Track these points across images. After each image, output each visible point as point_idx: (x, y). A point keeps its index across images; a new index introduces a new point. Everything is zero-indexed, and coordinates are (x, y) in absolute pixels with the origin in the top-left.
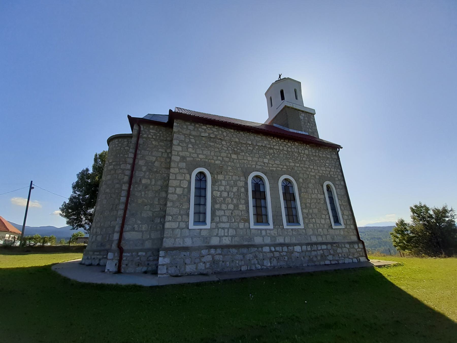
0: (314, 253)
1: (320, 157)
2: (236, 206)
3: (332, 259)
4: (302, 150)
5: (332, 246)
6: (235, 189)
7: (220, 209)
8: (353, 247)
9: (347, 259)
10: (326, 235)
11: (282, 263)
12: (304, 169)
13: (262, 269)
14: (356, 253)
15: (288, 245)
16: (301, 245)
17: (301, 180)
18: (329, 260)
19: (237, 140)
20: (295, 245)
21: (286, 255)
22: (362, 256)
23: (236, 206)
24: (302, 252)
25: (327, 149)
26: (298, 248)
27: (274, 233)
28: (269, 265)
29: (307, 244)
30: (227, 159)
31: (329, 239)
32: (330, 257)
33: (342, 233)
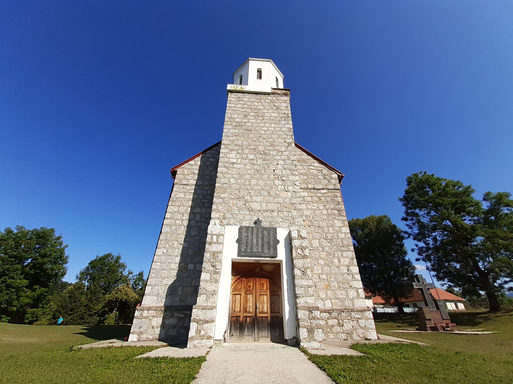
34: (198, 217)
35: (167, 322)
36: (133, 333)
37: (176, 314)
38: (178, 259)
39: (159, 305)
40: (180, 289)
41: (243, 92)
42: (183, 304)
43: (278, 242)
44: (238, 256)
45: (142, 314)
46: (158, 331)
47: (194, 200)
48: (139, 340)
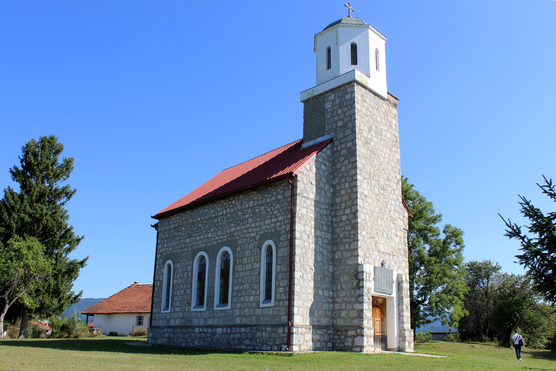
0: (232, 336)
1: (268, 203)
2: (185, 291)
3: (247, 344)
4: (245, 204)
5: (251, 328)
6: (185, 275)
7: (176, 295)
8: (276, 332)
9: (266, 346)
10: (251, 316)
11: (206, 344)
12: (245, 231)
13: (193, 347)
14: (279, 340)
15: (211, 327)
16: (222, 327)
17: (239, 249)
18: (245, 345)
19: (191, 221)
20: (218, 326)
21: (210, 337)
22: (285, 344)
23: (185, 291)
24: (223, 334)
25: (280, 184)
26: (219, 331)
27: (207, 314)
28: (198, 344)
29: (228, 327)
30: (183, 245)
31: (254, 321)
32: (247, 342)
33: (271, 312)
34: (320, 242)
35: (314, 337)
36: (295, 345)
37: (318, 331)
38: (312, 284)
39: (305, 324)
40: (316, 311)
41: (366, 88)
42: (319, 324)
43: (393, 282)
44: (374, 291)
45: (298, 331)
46: (311, 344)
47: (316, 220)
48: (300, 350)
